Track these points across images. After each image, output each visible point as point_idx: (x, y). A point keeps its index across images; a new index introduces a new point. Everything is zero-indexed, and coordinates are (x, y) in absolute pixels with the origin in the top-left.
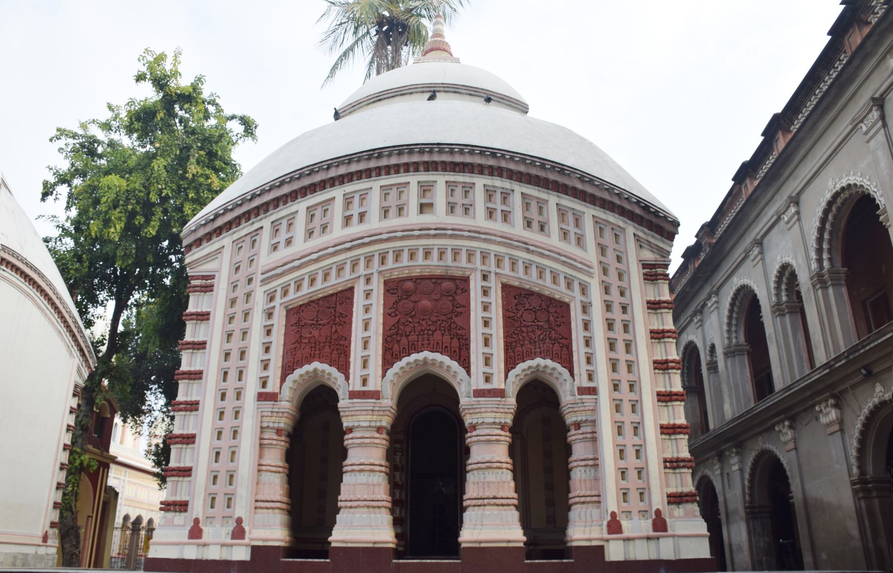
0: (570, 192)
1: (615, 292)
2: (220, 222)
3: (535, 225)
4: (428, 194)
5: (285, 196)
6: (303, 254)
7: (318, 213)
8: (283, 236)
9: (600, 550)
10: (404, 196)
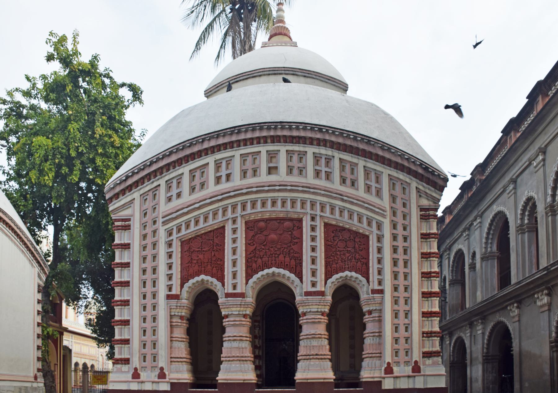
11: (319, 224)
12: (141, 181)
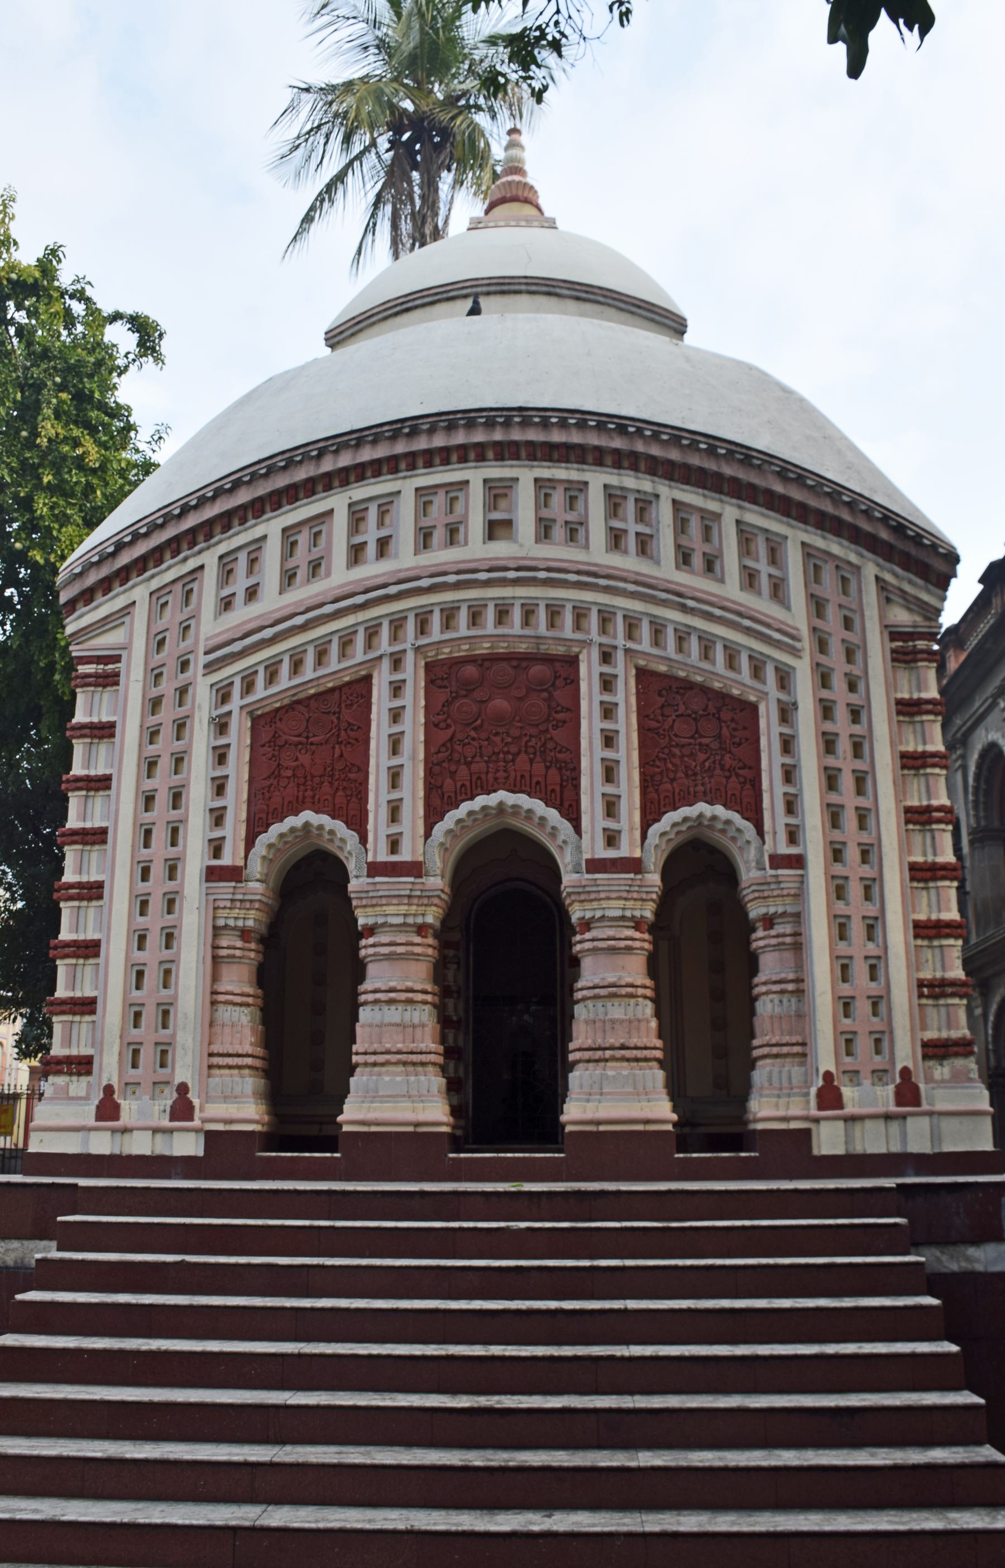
0: (761, 499)
1: (839, 683)
2: (125, 558)
3: (697, 561)
4: (502, 503)
5: (243, 507)
6: (277, 615)
7: (303, 538)
8: (240, 584)
10: (459, 508)
11: (621, 668)
12: (155, 557)
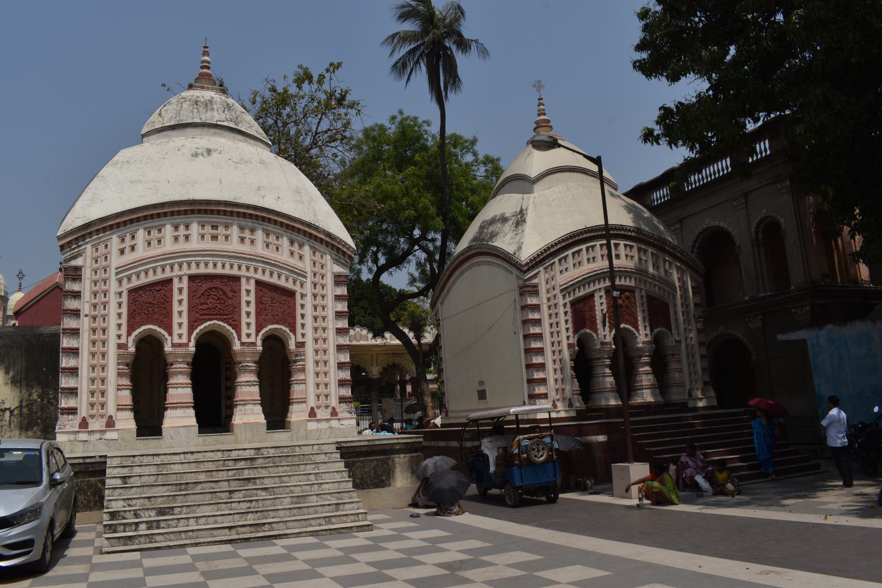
9: (686, 404)
11: (643, 293)
12: (544, 259)
